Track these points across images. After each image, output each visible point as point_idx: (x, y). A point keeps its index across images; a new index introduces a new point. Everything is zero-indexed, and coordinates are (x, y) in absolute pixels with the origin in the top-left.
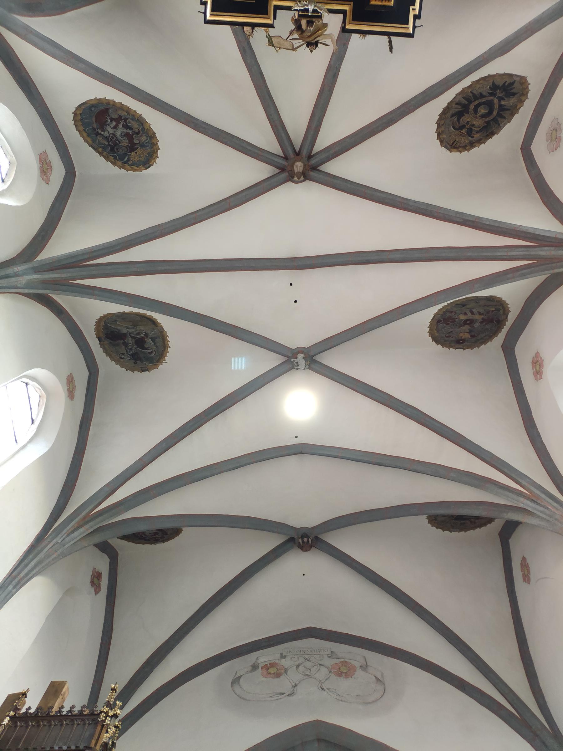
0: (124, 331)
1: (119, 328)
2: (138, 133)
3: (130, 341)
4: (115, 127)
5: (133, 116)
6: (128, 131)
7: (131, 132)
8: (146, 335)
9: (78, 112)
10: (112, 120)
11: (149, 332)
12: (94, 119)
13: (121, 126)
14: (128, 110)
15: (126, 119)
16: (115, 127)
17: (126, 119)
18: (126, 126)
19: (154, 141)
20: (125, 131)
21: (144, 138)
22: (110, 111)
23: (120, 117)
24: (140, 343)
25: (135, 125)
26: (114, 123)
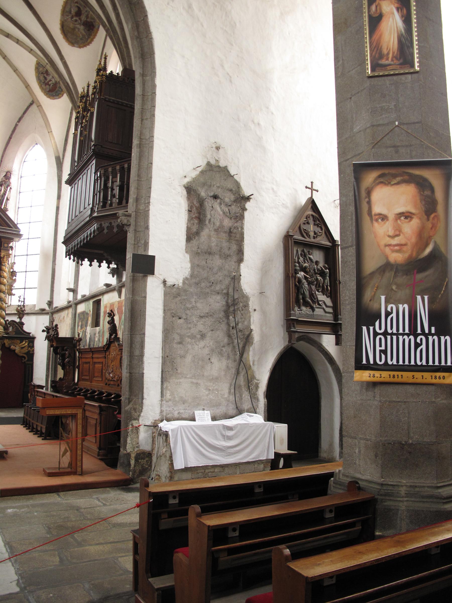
0: (82, 27)
1: (83, 32)
2: (42, 73)
3: (83, 18)
4: (50, 80)
5: (40, 83)
6: (46, 76)
7: (45, 75)
8: (72, 18)
9: (61, 96)
10: (50, 85)
11: (70, 19)
12: (57, 89)
13: (48, 80)
14: (41, 87)
15: (44, 83)
16: (50, 80)
17: (44, 83)
18: (46, 78)
19: (37, 66)
20: (47, 77)
21: (41, 69)
22: (48, 90)
23: (45, 85)
24: (79, 13)
25: (42, 78)
26: (50, 83)
